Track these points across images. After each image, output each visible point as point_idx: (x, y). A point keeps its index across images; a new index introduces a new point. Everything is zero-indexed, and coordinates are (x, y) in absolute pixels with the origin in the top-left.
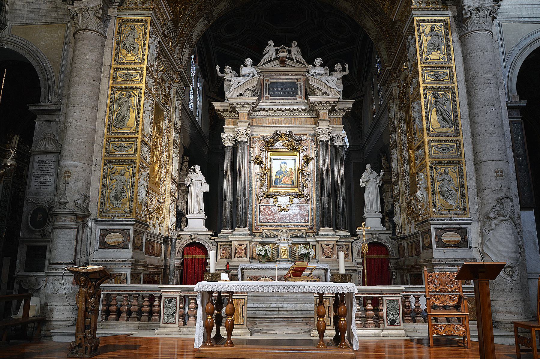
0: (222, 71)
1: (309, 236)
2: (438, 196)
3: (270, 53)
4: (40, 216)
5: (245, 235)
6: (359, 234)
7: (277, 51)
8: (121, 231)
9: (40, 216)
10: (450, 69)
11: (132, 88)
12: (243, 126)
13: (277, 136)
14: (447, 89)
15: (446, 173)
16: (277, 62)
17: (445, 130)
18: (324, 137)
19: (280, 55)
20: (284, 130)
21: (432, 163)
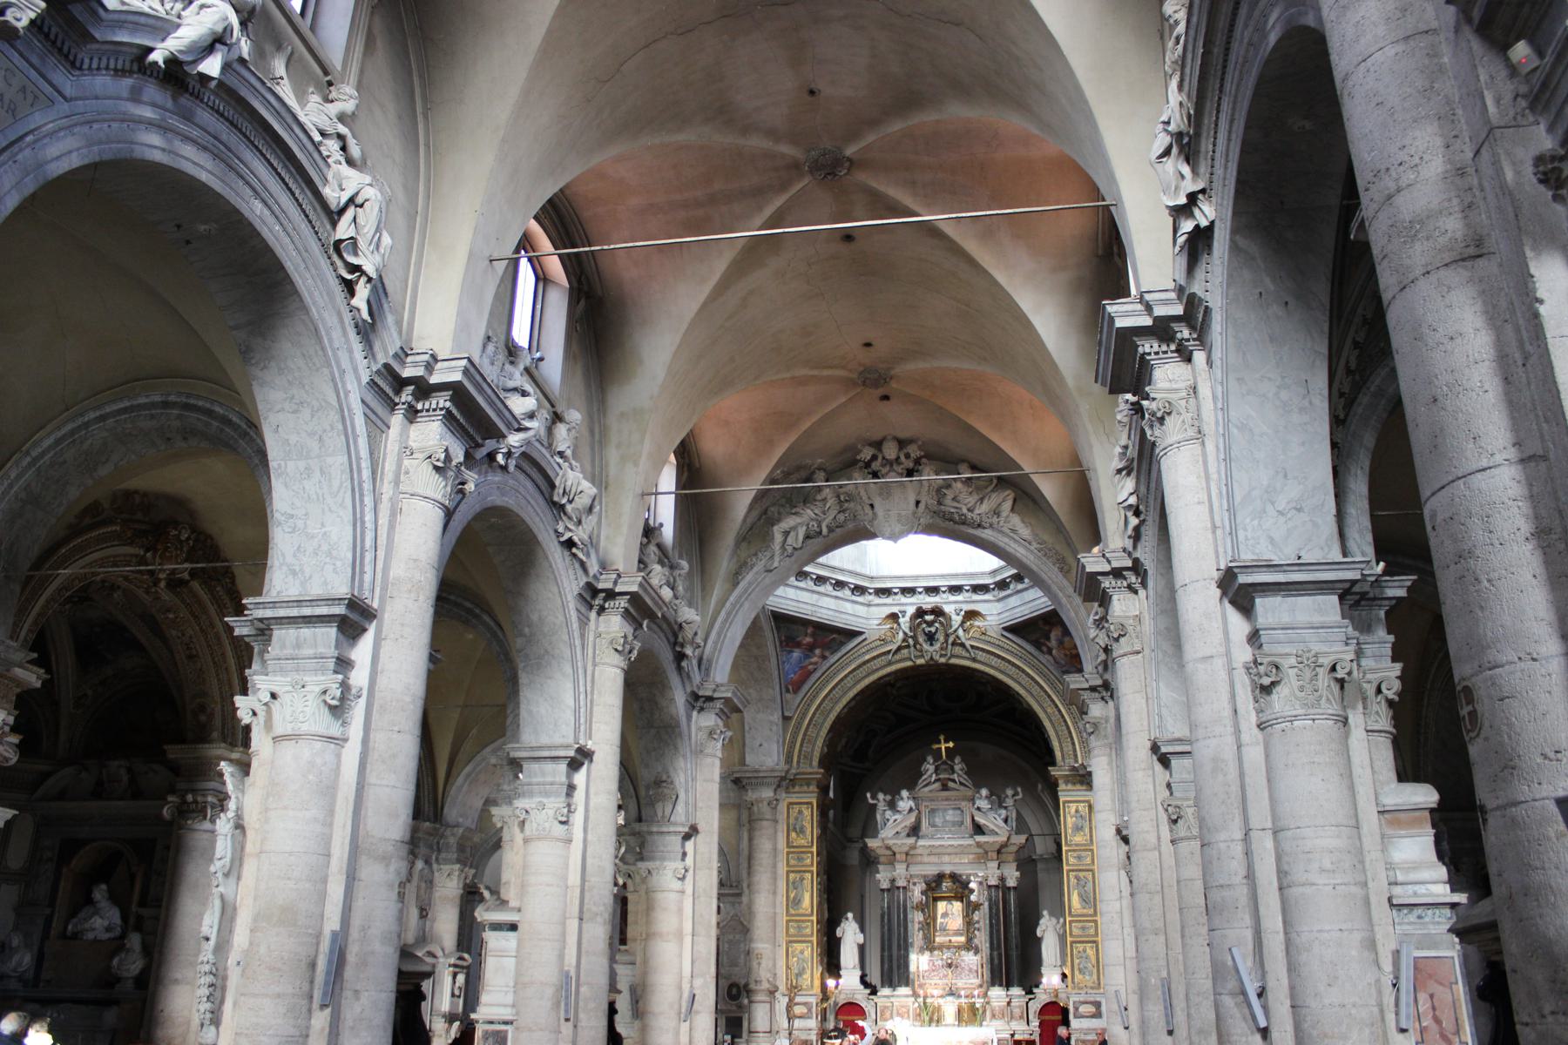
0: (874, 797)
1: (973, 997)
2: (1077, 972)
3: (929, 773)
4: (734, 991)
5: (907, 996)
6: (1032, 993)
7: (937, 770)
8: (805, 1004)
9: (734, 991)
10: (1092, 850)
11: (804, 871)
12: (900, 869)
13: (940, 877)
14: (1088, 870)
15: (1085, 951)
16: (937, 785)
17: (1085, 911)
18: (993, 882)
19: (941, 776)
20: (948, 870)
21: (1072, 943)
